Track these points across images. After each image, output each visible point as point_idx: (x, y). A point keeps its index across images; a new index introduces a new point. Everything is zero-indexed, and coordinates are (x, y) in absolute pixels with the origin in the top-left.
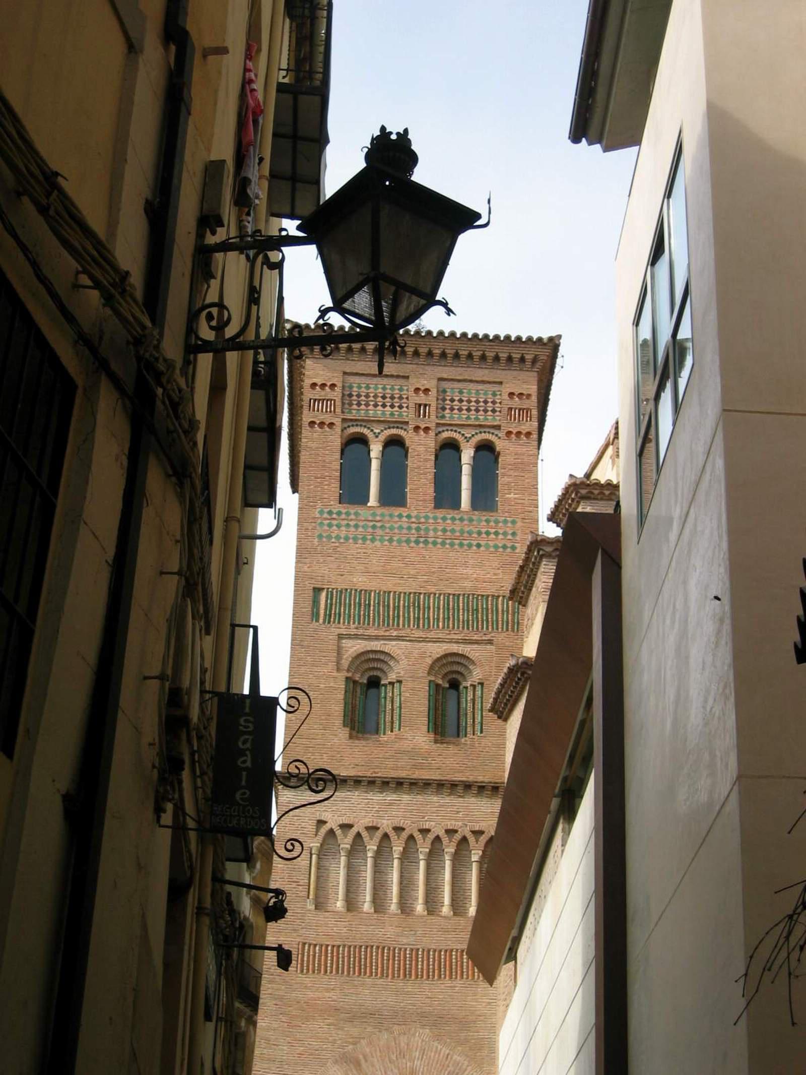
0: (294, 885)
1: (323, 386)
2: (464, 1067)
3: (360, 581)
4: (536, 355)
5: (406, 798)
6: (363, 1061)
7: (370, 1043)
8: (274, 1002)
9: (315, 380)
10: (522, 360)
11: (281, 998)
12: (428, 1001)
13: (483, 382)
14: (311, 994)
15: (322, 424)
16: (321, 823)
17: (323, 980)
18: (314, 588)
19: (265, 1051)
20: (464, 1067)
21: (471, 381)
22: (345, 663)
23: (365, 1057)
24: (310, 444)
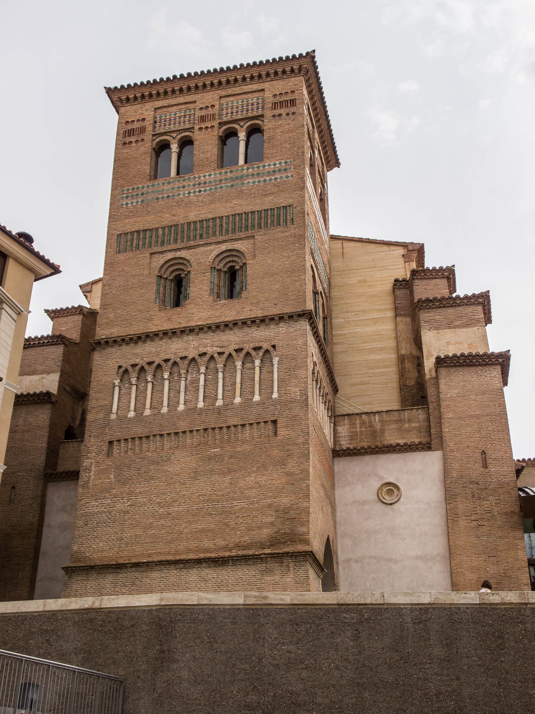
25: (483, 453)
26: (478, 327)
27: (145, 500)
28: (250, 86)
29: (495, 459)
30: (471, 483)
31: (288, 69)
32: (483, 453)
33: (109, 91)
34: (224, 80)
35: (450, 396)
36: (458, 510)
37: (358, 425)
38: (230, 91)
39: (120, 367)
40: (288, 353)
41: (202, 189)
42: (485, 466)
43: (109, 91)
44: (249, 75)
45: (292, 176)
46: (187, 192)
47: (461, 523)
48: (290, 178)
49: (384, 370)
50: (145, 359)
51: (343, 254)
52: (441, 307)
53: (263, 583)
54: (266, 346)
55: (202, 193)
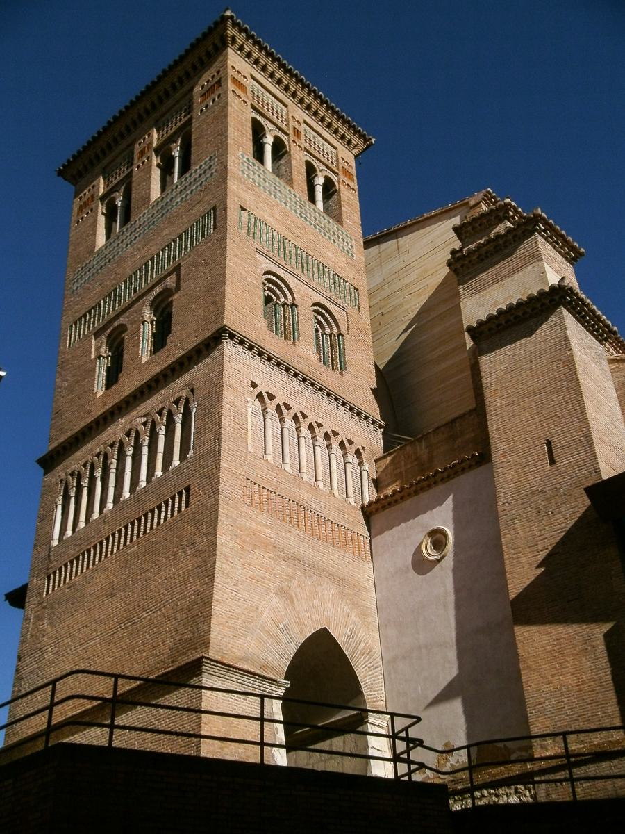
0: (238, 426)
1: (239, 72)
2: (359, 627)
3: (270, 220)
4: (358, 144)
5: (306, 393)
6: (295, 600)
7: (299, 585)
8: (230, 523)
9: (234, 66)
10: (349, 142)
11: (234, 520)
12: (331, 562)
13: (326, 141)
14: (255, 526)
15: (239, 96)
16: (254, 385)
17: (263, 518)
18: (241, 207)
19: (224, 566)
20: (359, 627)
21: (320, 135)
22: (260, 271)
23: (296, 594)
24: (233, 104)
25: (549, 443)
26: (534, 265)
27: (69, 640)
28: (181, 91)
29: (564, 447)
30: (533, 493)
31: (210, 48)
32: (549, 443)
33: (60, 173)
34: (155, 99)
35: (495, 376)
36: (519, 540)
37: (403, 463)
38: (163, 109)
39: (62, 480)
40: (205, 393)
41: (137, 235)
42: (552, 462)
43: (60, 173)
44: (176, 80)
45: (216, 171)
46: (124, 246)
47: (523, 560)
48: (215, 174)
49: (460, 377)
50: (80, 462)
51: (398, 249)
52: (482, 260)
53: (158, 720)
54: (184, 394)
55: (138, 239)
